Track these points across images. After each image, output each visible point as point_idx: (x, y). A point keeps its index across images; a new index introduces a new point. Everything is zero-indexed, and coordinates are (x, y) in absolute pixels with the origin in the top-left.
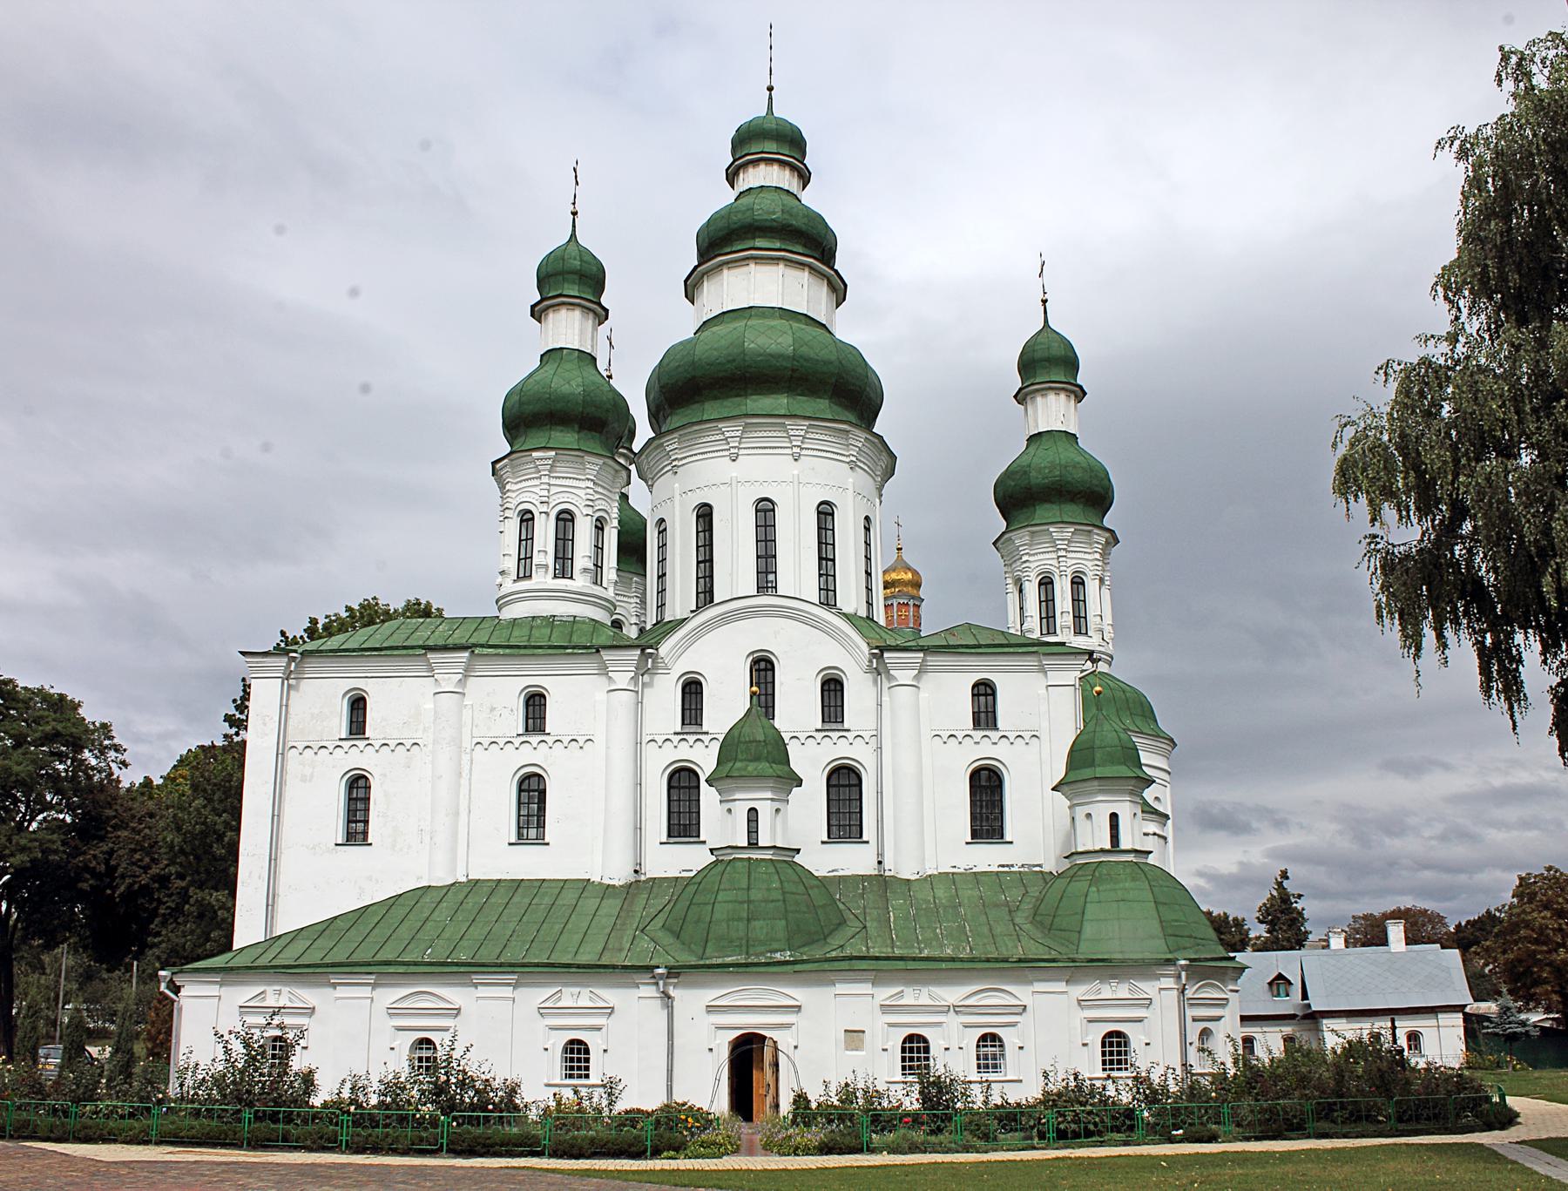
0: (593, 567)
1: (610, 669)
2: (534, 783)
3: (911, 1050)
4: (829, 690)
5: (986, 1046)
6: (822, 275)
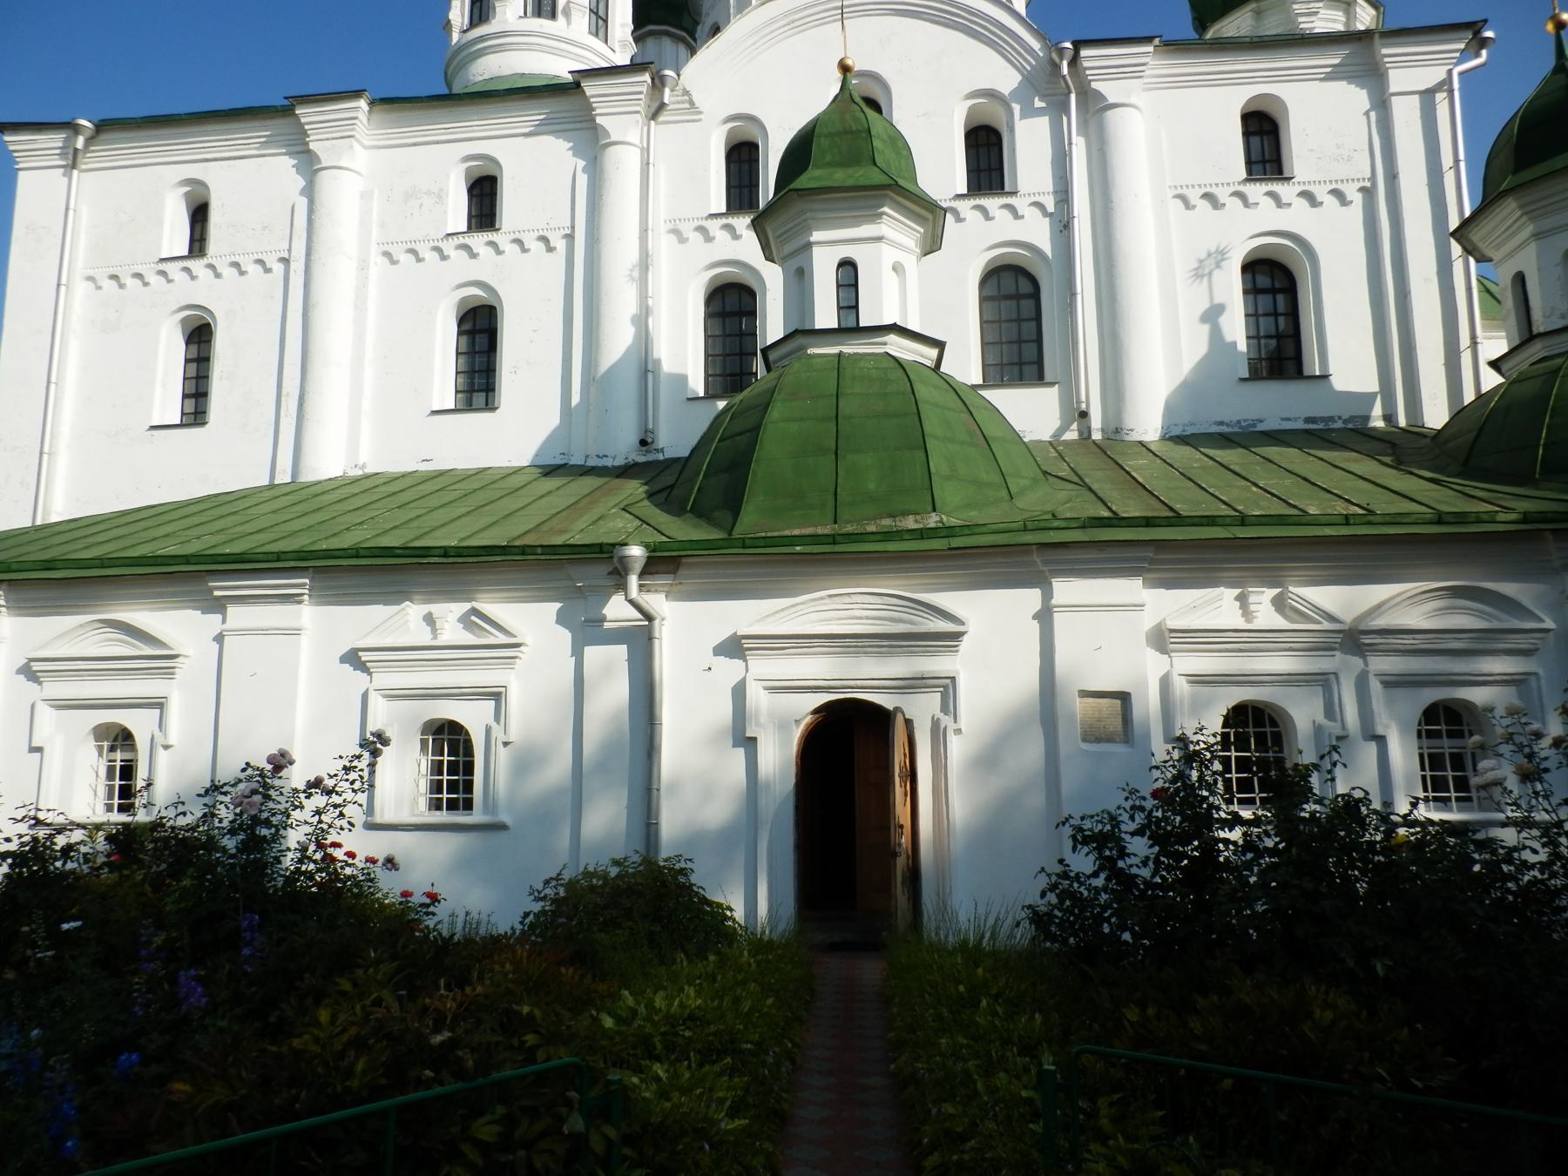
1: (598, 111)
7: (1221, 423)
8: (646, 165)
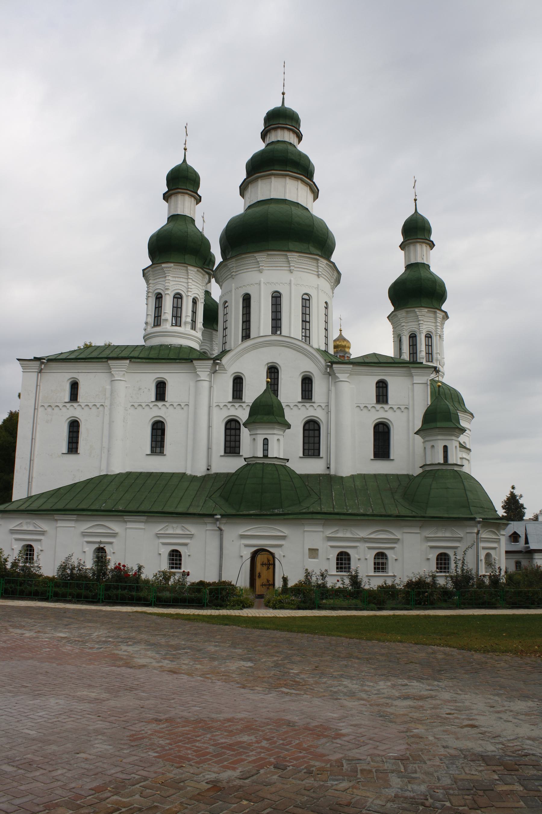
0: (191, 322)
1: (198, 370)
2: (159, 425)
3: (341, 560)
4: (305, 383)
5: (379, 558)
6: (307, 184)
8: (211, 387)
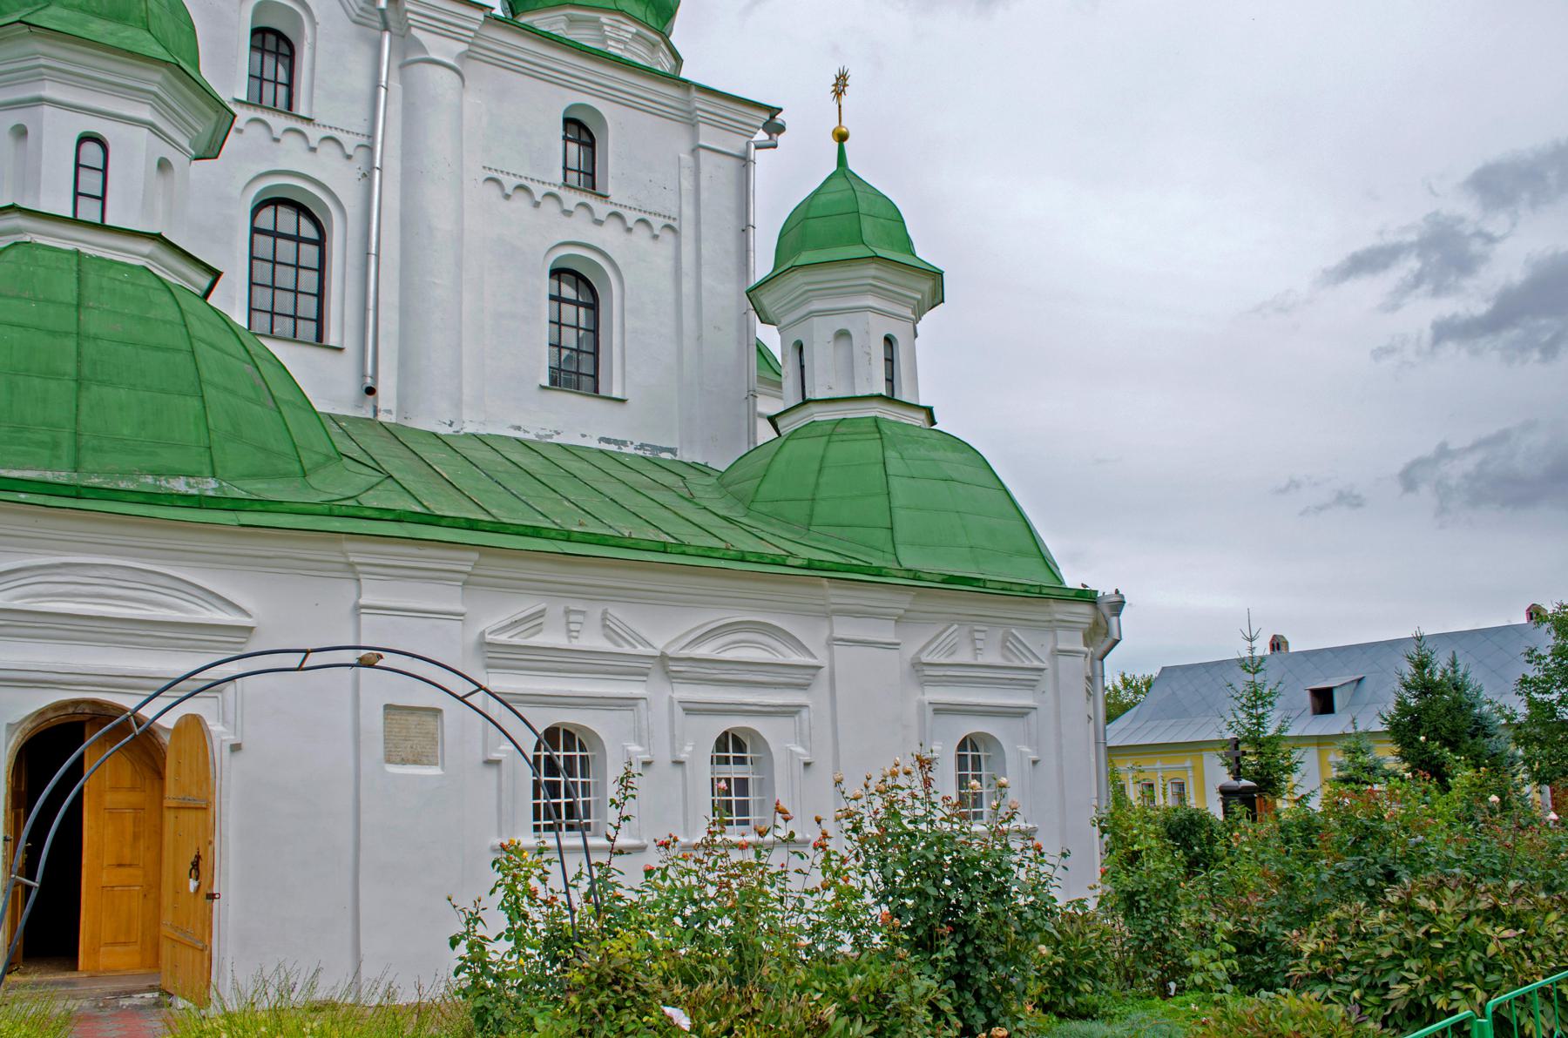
5: (727, 761)
7: (519, 428)
